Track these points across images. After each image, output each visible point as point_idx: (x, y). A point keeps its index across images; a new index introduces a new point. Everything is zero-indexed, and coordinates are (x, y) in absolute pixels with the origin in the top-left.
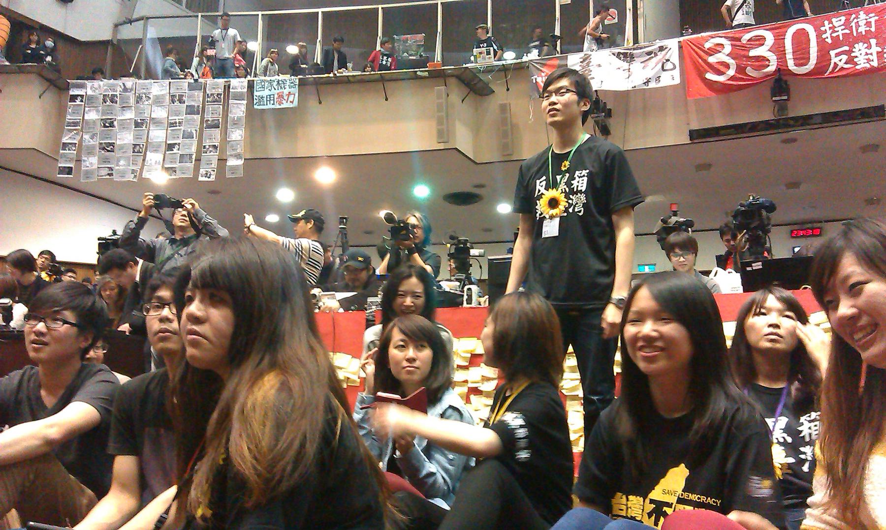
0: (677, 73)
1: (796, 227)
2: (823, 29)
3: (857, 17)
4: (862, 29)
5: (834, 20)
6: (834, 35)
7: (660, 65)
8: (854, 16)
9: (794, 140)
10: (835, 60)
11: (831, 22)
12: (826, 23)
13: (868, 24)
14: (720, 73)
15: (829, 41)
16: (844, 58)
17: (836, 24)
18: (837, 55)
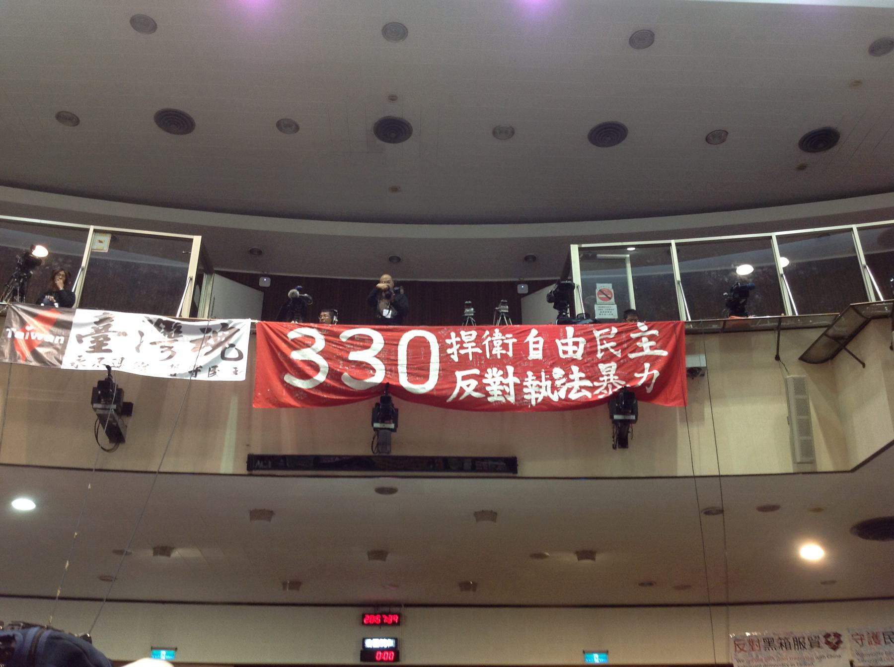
0: (242, 365)
2: (448, 341)
3: (491, 335)
4: (498, 351)
5: (463, 333)
6: (462, 352)
7: (219, 351)
8: (487, 333)
9: (392, 491)
10: (460, 384)
11: (458, 335)
12: (453, 334)
13: (505, 346)
14: (304, 376)
15: (455, 358)
16: (474, 383)
17: (465, 339)
18: (464, 378)
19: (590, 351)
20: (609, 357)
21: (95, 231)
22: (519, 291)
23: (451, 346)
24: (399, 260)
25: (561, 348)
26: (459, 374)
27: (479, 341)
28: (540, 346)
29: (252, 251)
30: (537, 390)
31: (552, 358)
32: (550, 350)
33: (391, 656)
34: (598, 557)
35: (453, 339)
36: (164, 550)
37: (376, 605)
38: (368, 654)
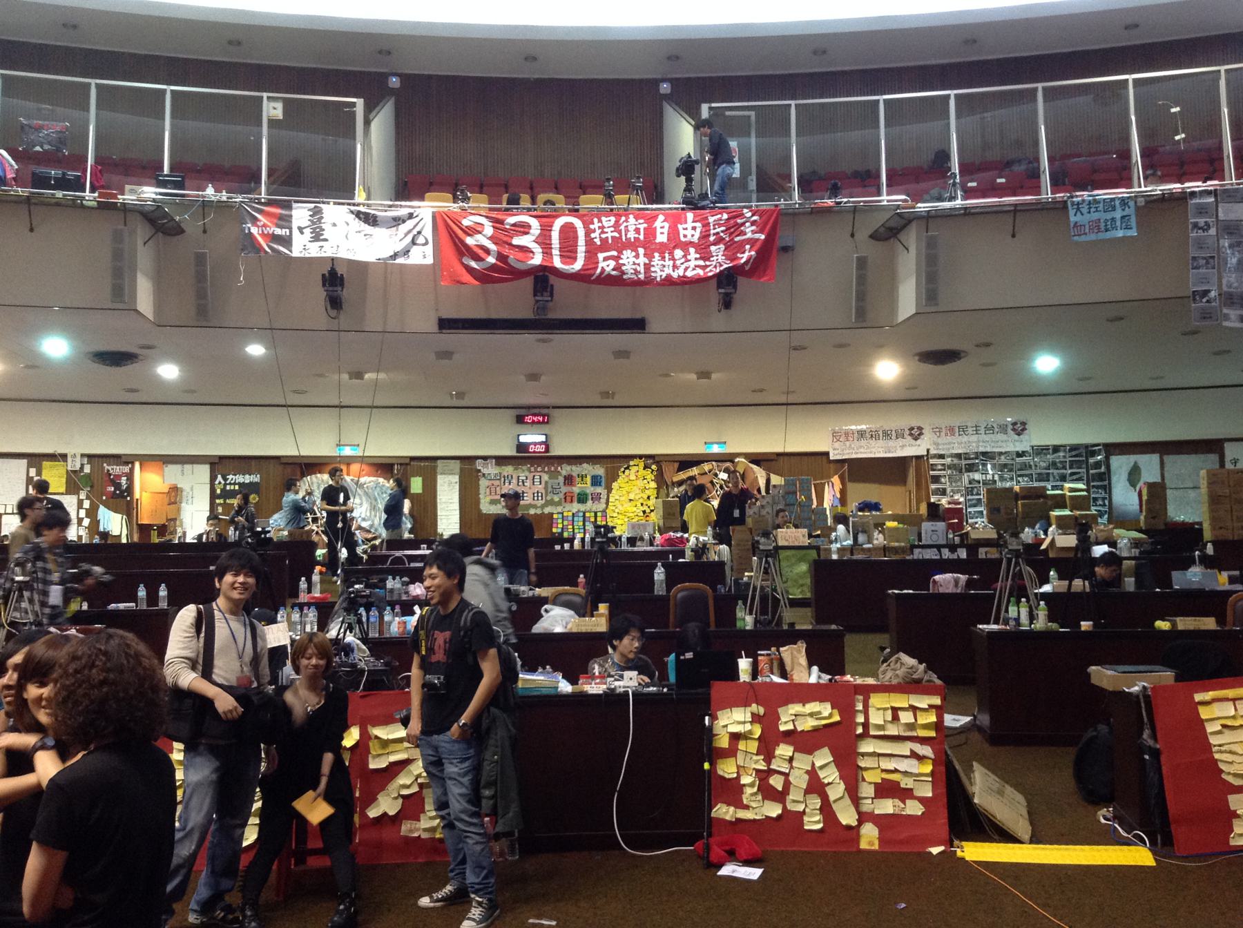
0: (429, 249)
1: (522, 412)
2: (592, 227)
3: (626, 221)
4: (632, 235)
5: (604, 219)
6: (604, 236)
7: (410, 237)
8: (623, 218)
10: (602, 264)
11: (600, 221)
12: (596, 220)
13: (637, 231)
14: (478, 259)
15: (598, 242)
16: (612, 263)
17: (606, 224)
18: (605, 259)
19: (705, 236)
20: (719, 241)
21: (268, 98)
22: (662, 91)
23: (594, 231)
24: (535, 59)
25: (682, 232)
26: (601, 256)
27: (616, 226)
28: (666, 230)
29: (380, 52)
30: (662, 268)
31: (675, 242)
32: (674, 233)
33: (541, 448)
34: (714, 376)
35: (596, 225)
36: (358, 375)
37: (529, 407)
38: (522, 447)
